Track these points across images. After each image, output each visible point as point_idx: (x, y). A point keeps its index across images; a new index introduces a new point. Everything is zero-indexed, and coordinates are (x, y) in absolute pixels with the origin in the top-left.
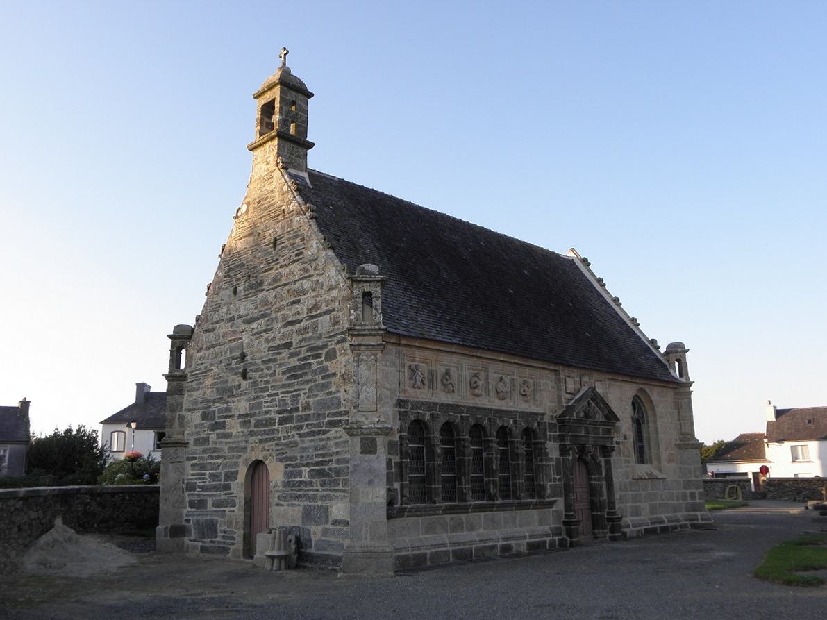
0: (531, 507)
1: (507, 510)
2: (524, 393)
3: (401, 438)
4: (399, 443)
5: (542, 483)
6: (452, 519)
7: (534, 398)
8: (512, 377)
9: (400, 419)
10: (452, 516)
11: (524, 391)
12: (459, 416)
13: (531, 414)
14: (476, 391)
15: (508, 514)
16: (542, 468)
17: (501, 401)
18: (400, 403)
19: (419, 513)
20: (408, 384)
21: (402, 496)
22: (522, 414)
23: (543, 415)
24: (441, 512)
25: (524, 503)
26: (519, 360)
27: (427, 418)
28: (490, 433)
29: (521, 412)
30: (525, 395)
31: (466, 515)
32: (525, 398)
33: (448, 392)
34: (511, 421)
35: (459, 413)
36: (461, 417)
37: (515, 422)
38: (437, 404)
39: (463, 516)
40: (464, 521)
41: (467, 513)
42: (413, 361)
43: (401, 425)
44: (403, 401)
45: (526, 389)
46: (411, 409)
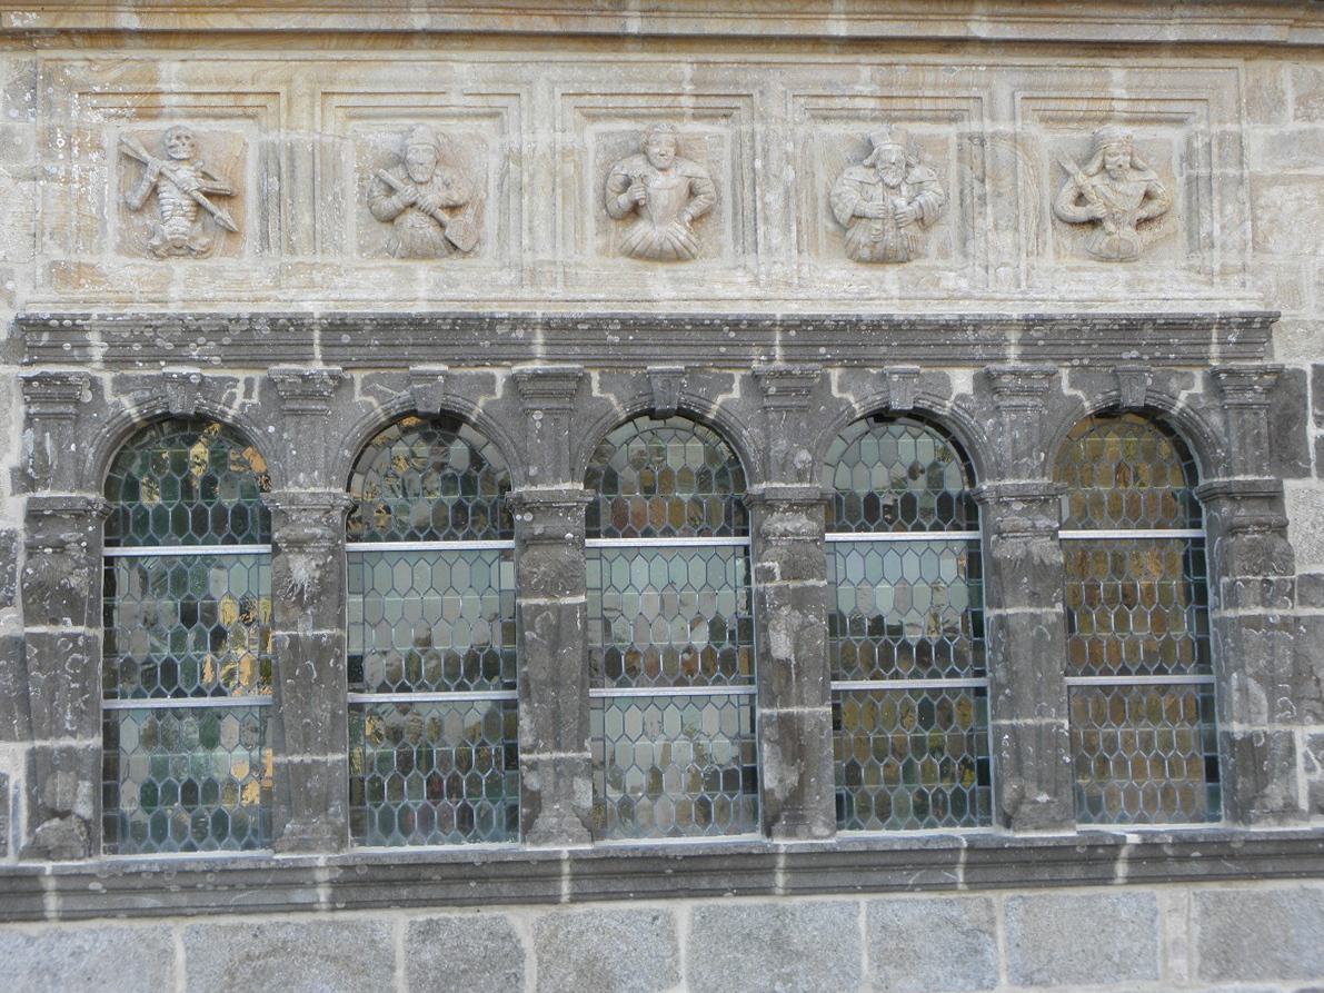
0: (1121, 869)
1: (902, 888)
2: (1081, 213)
3: (34, 516)
4: (22, 538)
5: (1238, 729)
6: (428, 932)
7: (1191, 234)
8: (974, 126)
9: (29, 421)
10: (422, 916)
11: (1080, 199)
12: (500, 375)
13: (1131, 326)
14: (641, 232)
15: (911, 908)
16: (1238, 638)
17: (866, 273)
18: (40, 336)
19: (148, 901)
20: (112, 239)
21: (42, 812)
22: (1050, 336)
23: (1255, 328)
24: (323, 894)
25: (1031, 848)
26: (995, 18)
27: (240, 396)
28: (766, 459)
29: (1029, 323)
30: (1094, 223)
31: (535, 913)
32: (1099, 240)
33: (413, 254)
34: (962, 380)
35: (496, 361)
36: (514, 381)
37: (987, 383)
38: (298, 324)
39: (522, 921)
40: (528, 944)
41: (554, 900)
42: (146, 113)
43: (39, 445)
44: (41, 325)
45: (1096, 184)
46: (109, 362)
